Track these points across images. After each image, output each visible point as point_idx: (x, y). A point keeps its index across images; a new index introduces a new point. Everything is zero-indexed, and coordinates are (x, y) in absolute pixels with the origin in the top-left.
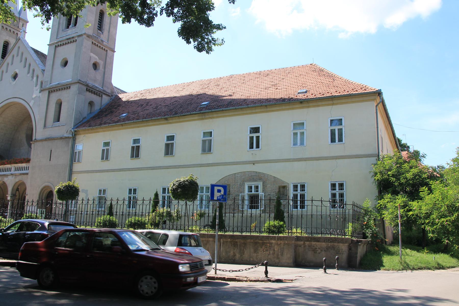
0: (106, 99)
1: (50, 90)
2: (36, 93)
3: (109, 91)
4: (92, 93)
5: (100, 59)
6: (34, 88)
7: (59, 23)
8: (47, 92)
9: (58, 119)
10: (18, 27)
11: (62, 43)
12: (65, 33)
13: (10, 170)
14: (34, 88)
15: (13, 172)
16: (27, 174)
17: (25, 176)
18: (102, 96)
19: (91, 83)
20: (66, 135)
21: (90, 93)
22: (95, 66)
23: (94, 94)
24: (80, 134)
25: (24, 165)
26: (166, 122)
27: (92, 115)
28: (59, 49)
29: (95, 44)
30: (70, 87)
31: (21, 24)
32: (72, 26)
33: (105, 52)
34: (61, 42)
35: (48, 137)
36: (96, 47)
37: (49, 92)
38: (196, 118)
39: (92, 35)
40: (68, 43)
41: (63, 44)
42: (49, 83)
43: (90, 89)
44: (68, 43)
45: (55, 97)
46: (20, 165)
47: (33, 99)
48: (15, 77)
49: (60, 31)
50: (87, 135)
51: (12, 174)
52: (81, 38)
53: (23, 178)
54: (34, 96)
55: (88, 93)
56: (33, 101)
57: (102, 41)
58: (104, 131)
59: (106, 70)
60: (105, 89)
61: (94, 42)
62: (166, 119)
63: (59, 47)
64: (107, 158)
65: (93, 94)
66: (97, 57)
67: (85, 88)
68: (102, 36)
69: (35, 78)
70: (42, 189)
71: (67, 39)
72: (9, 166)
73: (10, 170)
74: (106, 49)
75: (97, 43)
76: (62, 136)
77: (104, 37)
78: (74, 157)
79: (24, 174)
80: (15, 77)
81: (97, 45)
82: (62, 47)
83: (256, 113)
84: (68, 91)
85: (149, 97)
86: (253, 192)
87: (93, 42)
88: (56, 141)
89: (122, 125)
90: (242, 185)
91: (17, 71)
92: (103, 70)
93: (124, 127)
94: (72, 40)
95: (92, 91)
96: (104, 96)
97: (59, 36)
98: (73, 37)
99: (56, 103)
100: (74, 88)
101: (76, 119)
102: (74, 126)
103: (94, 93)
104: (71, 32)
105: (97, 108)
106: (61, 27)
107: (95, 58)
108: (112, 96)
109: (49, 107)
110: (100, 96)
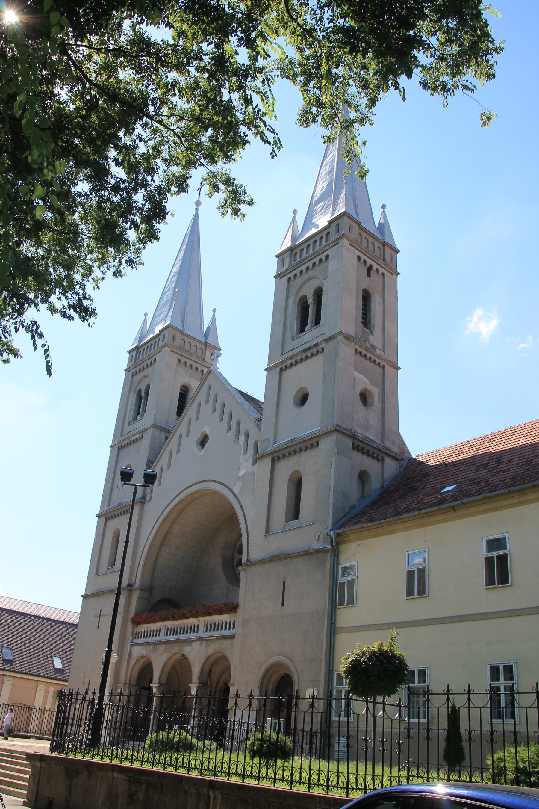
0: (391, 467)
1: (276, 455)
2: (245, 466)
3: (395, 449)
4: (363, 453)
5: (373, 383)
6: (242, 456)
7: (285, 327)
8: (269, 461)
9: (295, 512)
10: (204, 360)
11: (293, 361)
13: (195, 629)
14: (242, 456)
15: (201, 633)
16: (232, 637)
17: (228, 641)
18: (383, 460)
19: (360, 432)
20: (316, 546)
21: (360, 454)
22: (364, 397)
23: (368, 455)
24: (350, 541)
25: (225, 618)
27: (367, 501)
28: (288, 373)
29: (361, 353)
30: (318, 444)
31: (208, 353)
32: (312, 327)
33: (381, 370)
34: (290, 358)
36: (363, 359)
37: (273, 460)
39: (353, 335)
40: (307, 357)
41: (296, 362)
42: (272, 442)
43: (361, 446)
45: (285, 469)
47: (239, 479)
48: (203, 441)
49: (288, 340)
50: (365, 542)
51: (200, 639)
52: (333, 343)
54: (242, 472)
55: (355, 452)
56: (239, 484)
57: (373, 346)
58: (407, 529)
59: (387, 406)
60: (388, 444)
61: (359, 349)
65: (365, 457)
66: (366, 380)
67: (349, 442)
68: (371, 337)
69: (242, 438)
70: (267, 671)
71: (304, 351)
72: (192, 621)
73: (195, 629)
74: (382, 363)
75: (364, 352)
76: (307, 549)
77: (375, 339)
78: (340, 594)
79: (224, 637)
80: (203, 441)
81: (365, 356)
82: (294, 369)
84: (314, 452)
85: (494, 449)
87: (356, 350)
88: (295, 561)
89: (453, 508)
91: (207, 430)
92: (380, 406)
93: (458, 513)
95: (363, 449)
96: (387, 460)
97: (287, 349)
98: (316, 345)
99: (290, 481)
100: (328, 444)
101: (336, 509)
102: (334, 524)
103: (368, 454)
104: (311, 336)
105: (375, 484)
106: (288, 332)
107: (363, 382)
108: (402, 460)
109: (275, 490)
110: (378, 460)
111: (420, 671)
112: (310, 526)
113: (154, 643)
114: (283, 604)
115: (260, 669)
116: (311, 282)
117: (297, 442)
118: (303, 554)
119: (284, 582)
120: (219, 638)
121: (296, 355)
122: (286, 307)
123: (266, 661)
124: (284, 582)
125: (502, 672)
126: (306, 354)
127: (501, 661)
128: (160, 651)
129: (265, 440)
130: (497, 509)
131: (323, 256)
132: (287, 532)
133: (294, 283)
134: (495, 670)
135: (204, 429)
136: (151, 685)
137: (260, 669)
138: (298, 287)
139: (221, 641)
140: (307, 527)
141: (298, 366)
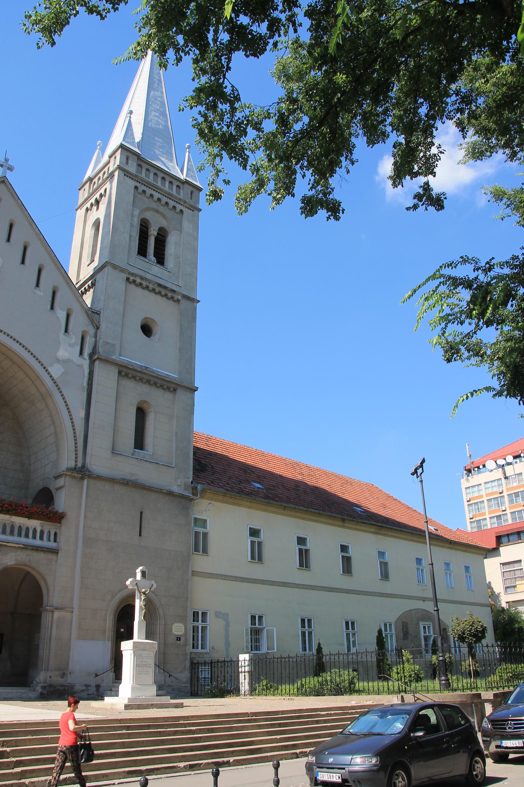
7: (130, 236)
11: (145, 284)
20: (175, 489)
26: (341, 524)
34: (142, 278)
35: (128, 477)
38: (372, 530)
40: (159, 293)
41: (141, 284)
42: (117, 352)
46: (18, 520)
47: (58, 361)
50: (215, 503)
53: (38, 562)
54: (62, 354)
58: (249, 507)
62: (343, 520)
63: (133, 286)
64: (260, 559)
71: (160, 285)
76: (168, 488)
83: (400, 538)
84: (168, 395)
86: (427, 634)
89: (285, 508)
90: (417, 625)
93: (285, 512)
94: (170, 295)
98: (173, 291)
111: (202, 613)
112: (170, 468)
114: (140, 535)
115: (113, 597)
116: (157, 215)
117: (156, 375)
118: (165, 493)
119: (141, 513)
120: (26, 547)
121: (150, 281)
122: (133, 216)
124: (141, 513)
125: (350, 625)
126: (161, 289)
127: (349, 618)
129: (108, 343)
130: (304, 519)
131: (179, 207)
132: (142, 462)
133: (139, 196)
134: (253, 618)
138: (145, 206)
139: (29, 552)
140: (166, 467)
141: (146, 292)
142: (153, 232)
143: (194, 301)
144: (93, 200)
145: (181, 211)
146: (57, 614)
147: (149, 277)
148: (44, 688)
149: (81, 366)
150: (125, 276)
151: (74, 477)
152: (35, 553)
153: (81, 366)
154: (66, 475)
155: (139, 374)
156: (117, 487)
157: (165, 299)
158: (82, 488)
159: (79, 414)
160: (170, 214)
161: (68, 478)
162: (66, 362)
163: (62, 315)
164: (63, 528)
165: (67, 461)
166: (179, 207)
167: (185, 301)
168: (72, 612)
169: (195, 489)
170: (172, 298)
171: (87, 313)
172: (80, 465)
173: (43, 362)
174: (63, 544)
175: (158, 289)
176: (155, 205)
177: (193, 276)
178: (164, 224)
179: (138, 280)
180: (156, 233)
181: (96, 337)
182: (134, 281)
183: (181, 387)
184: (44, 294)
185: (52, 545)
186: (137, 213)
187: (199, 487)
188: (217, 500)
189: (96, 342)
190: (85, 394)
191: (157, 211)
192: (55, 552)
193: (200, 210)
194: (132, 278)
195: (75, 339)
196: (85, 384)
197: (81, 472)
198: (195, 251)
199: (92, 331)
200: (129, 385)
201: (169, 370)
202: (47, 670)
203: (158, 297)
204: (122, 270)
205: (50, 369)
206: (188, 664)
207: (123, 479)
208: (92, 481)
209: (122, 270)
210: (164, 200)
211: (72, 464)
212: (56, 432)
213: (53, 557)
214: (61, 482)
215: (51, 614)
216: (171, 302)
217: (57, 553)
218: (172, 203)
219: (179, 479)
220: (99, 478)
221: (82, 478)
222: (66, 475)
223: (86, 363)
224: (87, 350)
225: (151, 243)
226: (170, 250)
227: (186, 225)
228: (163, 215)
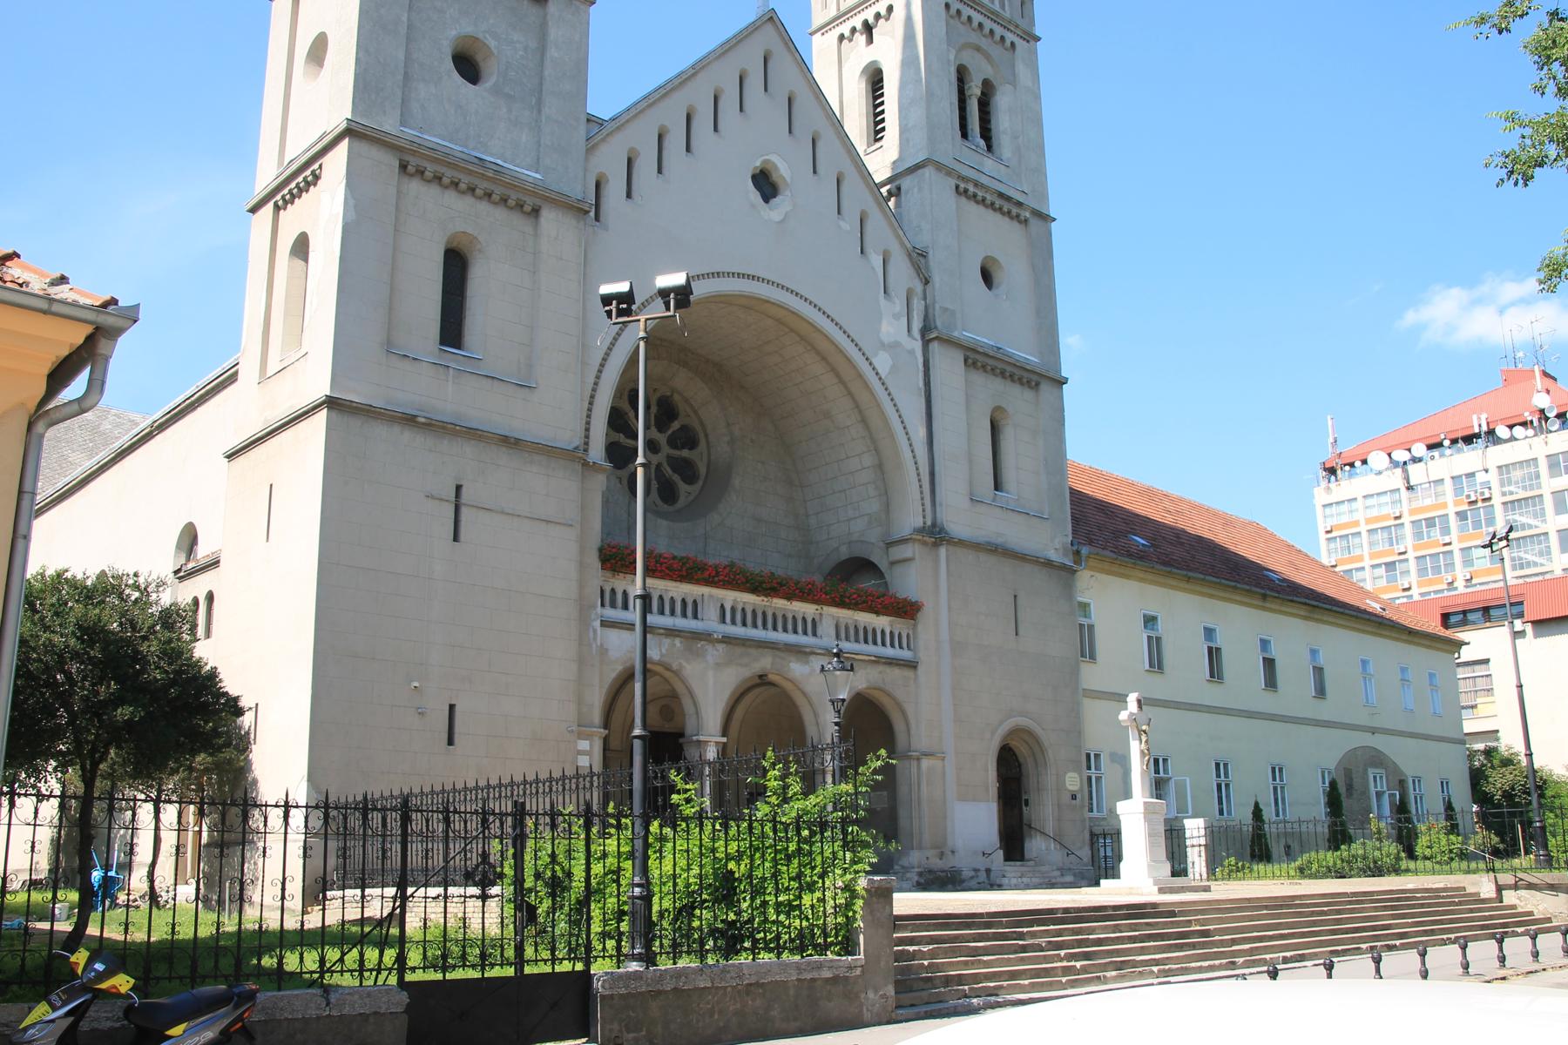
12: (977, 157)
25: (882, 622)
34: (976, 184)
44: (992, 204)
47: (883, 346)
48: (765, 184)
62: (1264, 597)
64: (1160, 667)
71: (1001, 195)
73: (813, 627)
80: (765, 184)
84: (1028, 394)
89: (1189, 579)
91: (783, 170)
94: (1015, 211)
98: (1019, 204)
113: (696, 636)
115: (993, 734)
116: (978, 56)
123: (1001, 723)
128: (710, 659)
130: (1211, 596)
131: (1010, 37)
135: (774, 158)
136: (724, 740)
137: (993, 734)
139: (881, 668)
141: (981, 209)
142: (975, 90)
143: (1046, 218)
144: (857, 22)
145: (1013, 44)
146: (925, 763)
147: (984, 180)
148: (920, 874)
149: (912, 352)
150: (952, 182)
151: (925, 543)
152: (888, 670)
153: (912, 352)
154: (915, 540)
155: (991, 362)
156: (983, 557)
157: (1007, 219)
158: (937, 561)
159: (920, 433)
160: (996, 51)
161: (917, 546)
162: (893, 347)
163: (877, 261)
164: (920, 627)
165: (911, 518)
166: (1010, 37)
167: (1027, 215)
168: (943, 759)
169: (1078, 553)
170: (1018, 216)
171: (909, 255)
172: (929, 523)
173: (865, 349)
174: (925, 656)
175: (998, 202)
176: (974, 38)
177: (1040, 171)
178: (987, 71)
179: (971, 189)
180: (979, 93)
181: (925, 298)
182: (966, 191)
183: (1041, 380)
184: (849, 225)
185: (905, 654)
186: (952, 57)
187: (1085, 551)
188: (1102, 571)
189: (926, 307)
190: (923, 400)
191: (978, 49)
192: (912, 665)
193: (1039, 39)
194: (962, 186)
195: (899, 305)
196: (921, 384)
197: (935, 535)
198: (1037, 122)
199: (919, 287)
200: (979, 378)
201: (1025, 352)
202: (920, 848)
203: (998, 216)
204: (950, 172)
205: (874, 361)
206: (1087, 836)
207: (989, 543)
208: (951, 548)
209: (950, 172)
210: (988, 25)
211: (919, 522)
212: (880, 467)
213: (909, 673)
214: (906, 551)
215: (914, 763)
216: (1015, 223)
217: (915, 667)
218: (999, 31)
219: (1052, 540)
220: (961, 543)
221: (936, 545)
222: (915, 540)
223: (917, 346)
224: (917, 325)
225: (975, 110)
226: (1003, 122)
227: (1022, 70)
228: (988, 57)
